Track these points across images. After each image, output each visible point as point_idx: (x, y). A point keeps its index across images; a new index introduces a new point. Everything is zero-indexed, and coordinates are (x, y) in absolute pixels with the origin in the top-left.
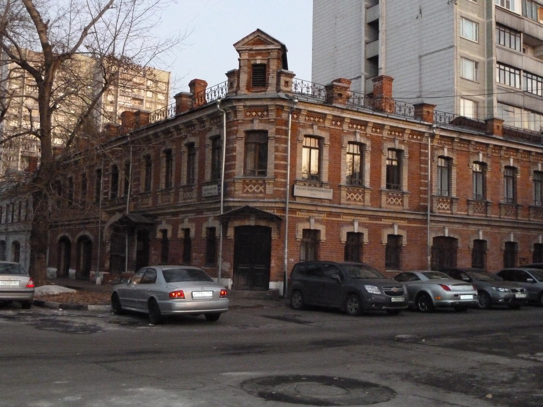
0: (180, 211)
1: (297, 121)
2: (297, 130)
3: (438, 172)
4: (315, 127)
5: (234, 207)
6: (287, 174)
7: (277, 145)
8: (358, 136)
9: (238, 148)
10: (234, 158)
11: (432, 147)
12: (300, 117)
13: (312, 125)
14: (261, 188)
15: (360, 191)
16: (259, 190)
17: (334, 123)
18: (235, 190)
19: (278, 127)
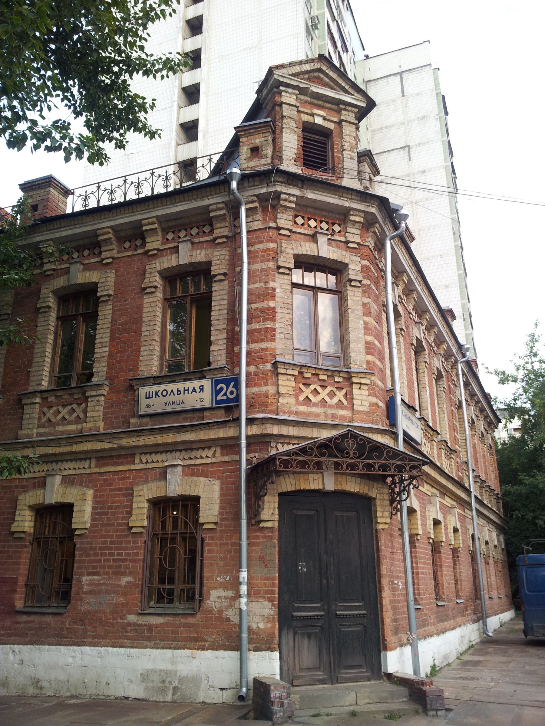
5: (279, 437)
10: (270, 314)
14: (340, 395)
16: (335, 400)
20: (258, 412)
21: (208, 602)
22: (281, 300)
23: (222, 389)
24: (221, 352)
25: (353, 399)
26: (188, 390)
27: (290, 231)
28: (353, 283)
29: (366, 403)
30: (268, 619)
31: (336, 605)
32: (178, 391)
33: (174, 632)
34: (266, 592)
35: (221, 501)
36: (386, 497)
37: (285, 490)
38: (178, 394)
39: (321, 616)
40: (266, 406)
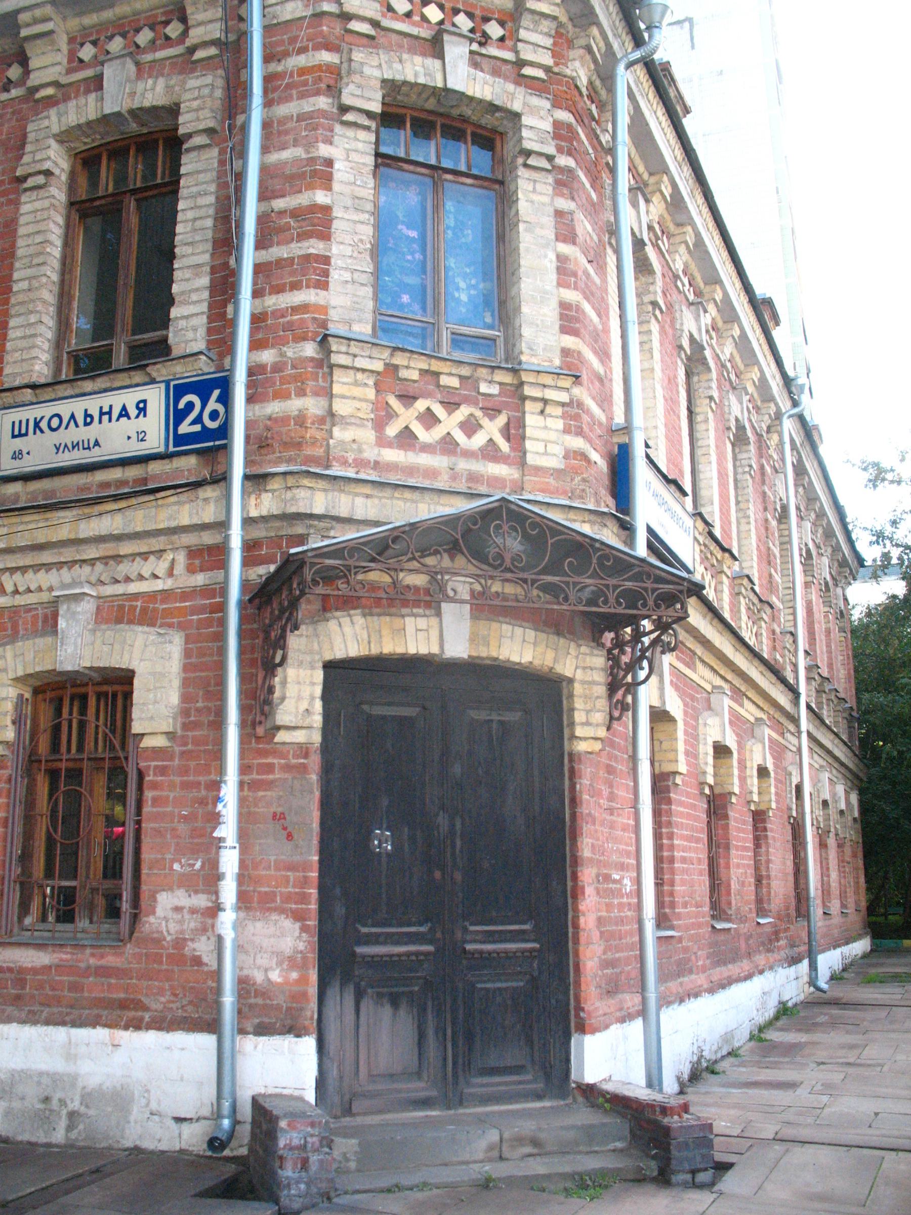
10: (318, 222)
14: (492, 429)
16: (479, 440)
20: (279, 461)
21: (152, 919)
22: (347, 190)
23: (190, 406)
24: (195, 321)
25: (523, 438)
26: (109, 413)
27: (375, 24)
28: (532, 161)
29: (558, 450)
30: (292, 962)
31: (465, 930)
32: (87, 415)
33: (75, 987)
34: (288, 898)
35: (185, 683)
36: (600, 677)
38: (86, 424)
39: (427, 954)
40: (299, 445)
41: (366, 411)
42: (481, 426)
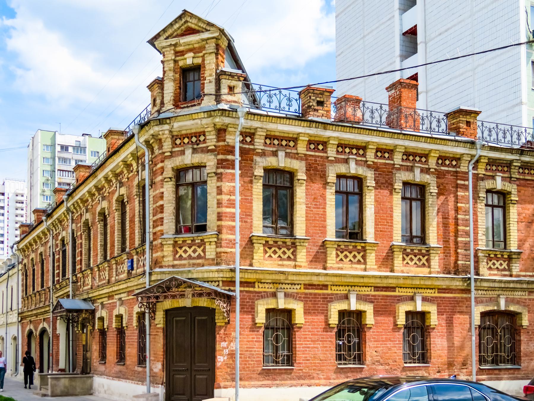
0: (113, 291)
1: (252, 147)
2: (252, 161)
3: (487, 214)
4: (281, 154)
6: (234, 227)
7: (219, 184)
8: (352, 164)
9: (165, 195)
11: (476, 176)
12: (256, 140)
13: (276, 151)
14: (199, 251)
15: (359, 248)
16: (197, 254)
17: (312, 146)
18: (163, 257)
19: (220, 157)
29: (214, 253)
37: (166, 308)
41: (171, 253)
42: (197, 251)
